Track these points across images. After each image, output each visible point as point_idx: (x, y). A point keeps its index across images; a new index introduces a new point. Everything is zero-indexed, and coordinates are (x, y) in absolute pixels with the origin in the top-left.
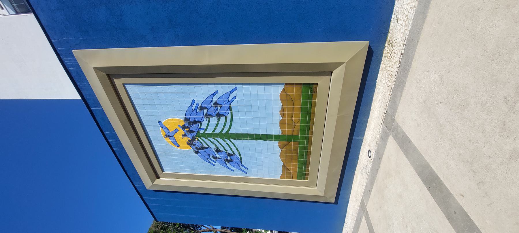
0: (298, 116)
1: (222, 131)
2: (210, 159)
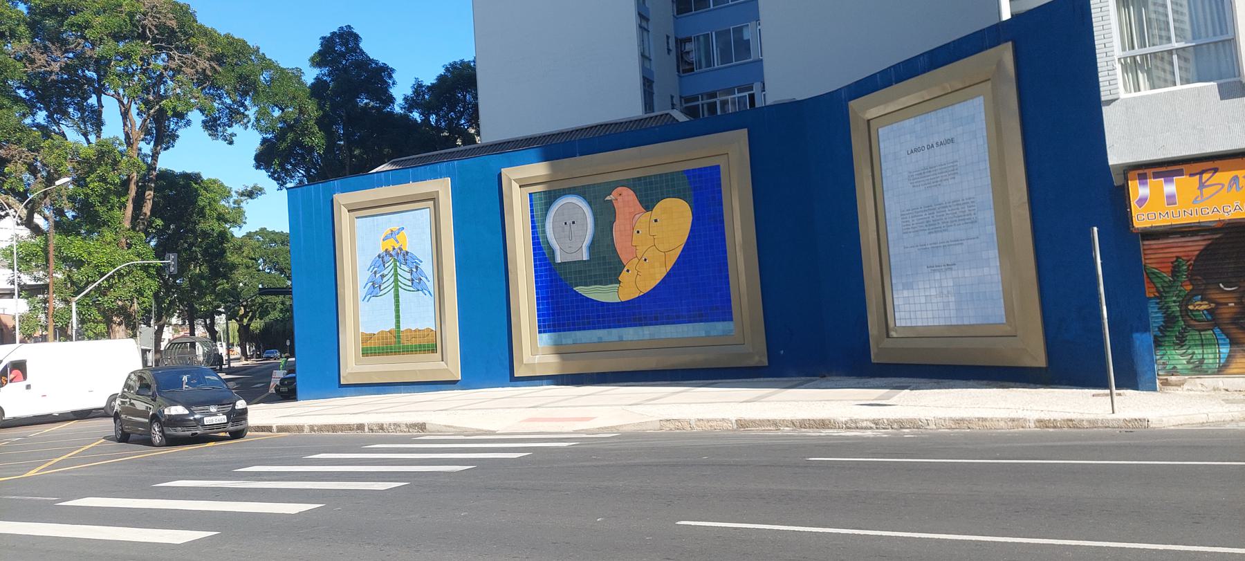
0: (415, 342)
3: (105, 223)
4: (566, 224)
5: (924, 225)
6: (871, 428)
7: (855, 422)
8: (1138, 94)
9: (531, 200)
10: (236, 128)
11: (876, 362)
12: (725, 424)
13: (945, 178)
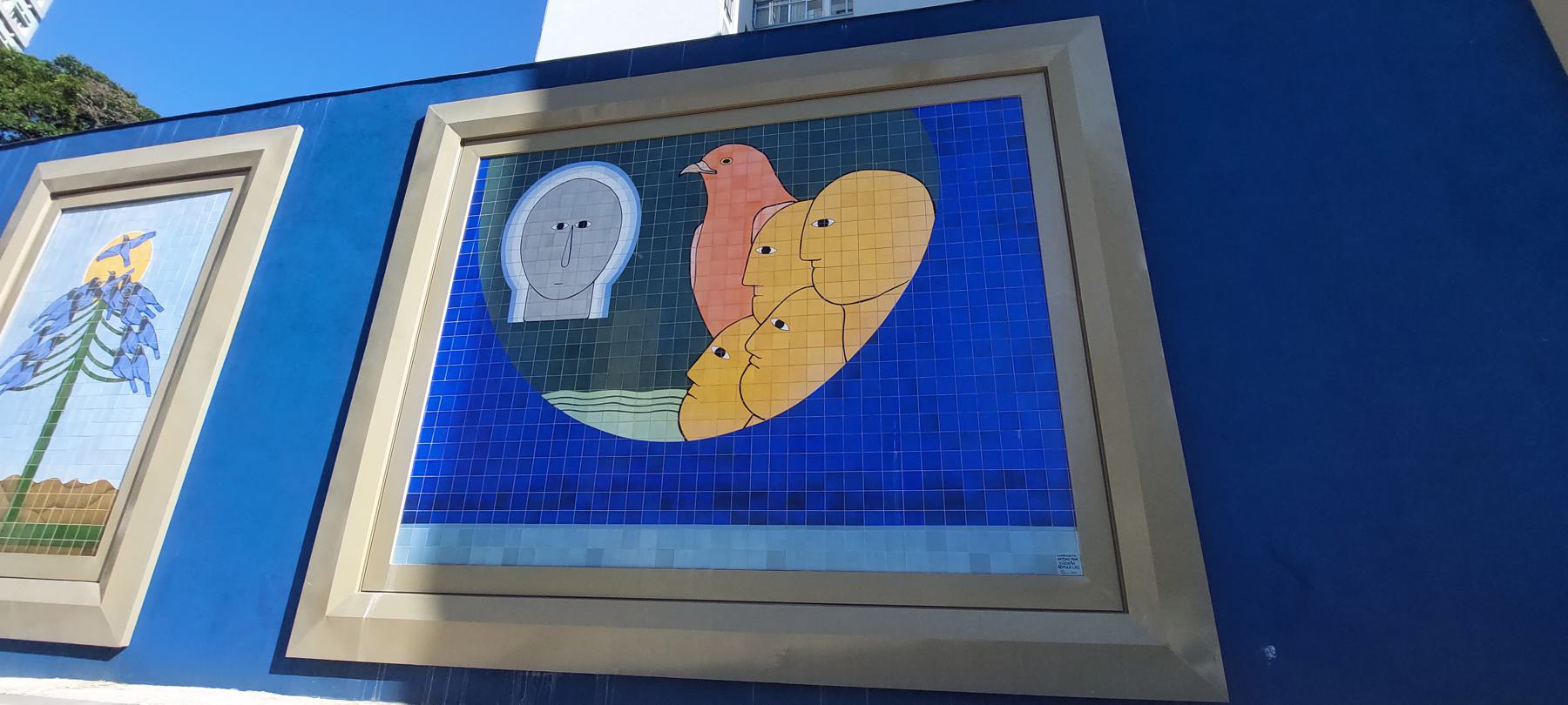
1: (92, 359)
2: (46, 321)
4: (560, 226)
9: (482, 174)
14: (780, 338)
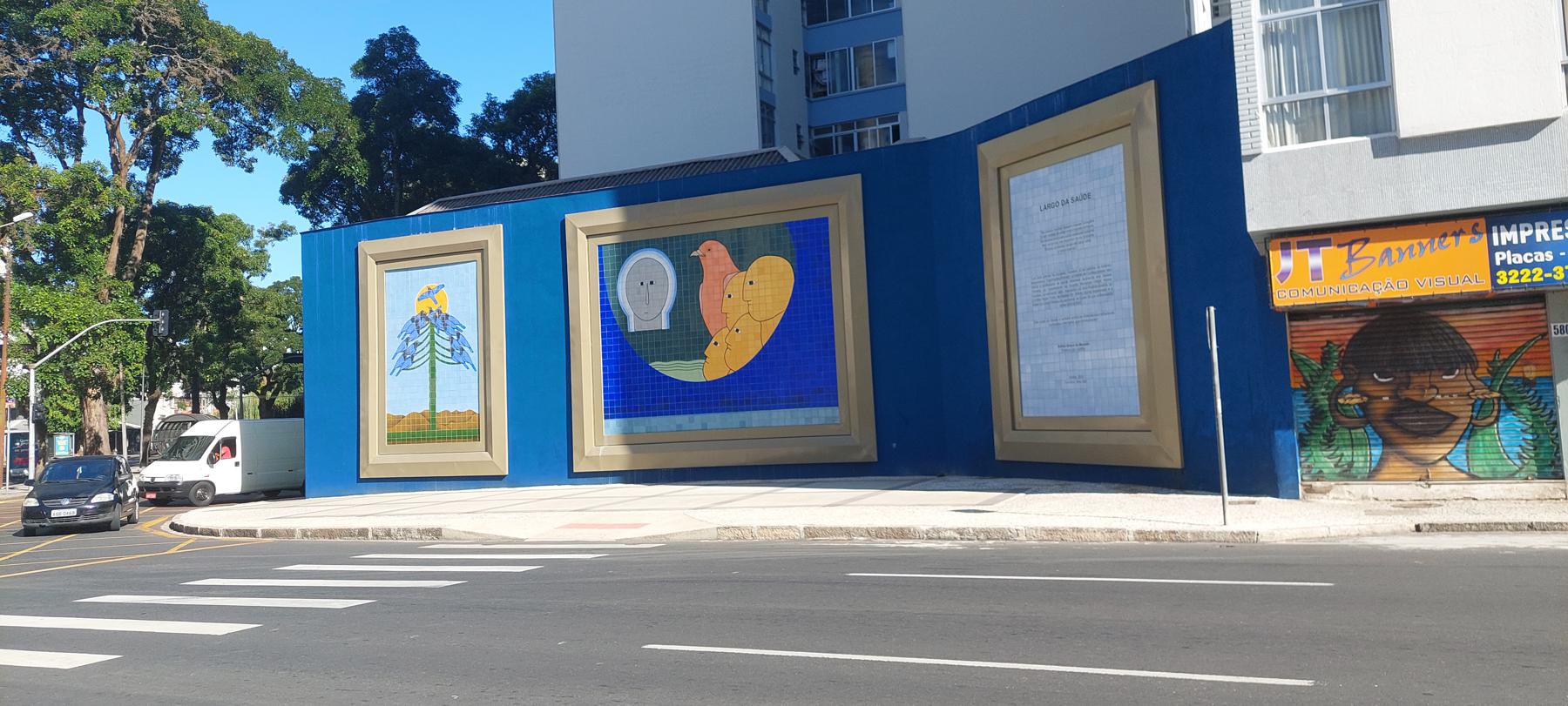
0: (454, 427)
3: (80, 270)
4: (642, 284)
5: (1056, 296)
6: (955, 539)
7: (937, 531)
8: (1284, 148)
9: (600, 254)
10: (257, 152)
11: (1000, 459)
12: (792, 533)
13: (1079, 240)
14: (738, 337)
